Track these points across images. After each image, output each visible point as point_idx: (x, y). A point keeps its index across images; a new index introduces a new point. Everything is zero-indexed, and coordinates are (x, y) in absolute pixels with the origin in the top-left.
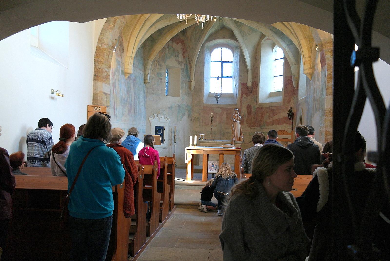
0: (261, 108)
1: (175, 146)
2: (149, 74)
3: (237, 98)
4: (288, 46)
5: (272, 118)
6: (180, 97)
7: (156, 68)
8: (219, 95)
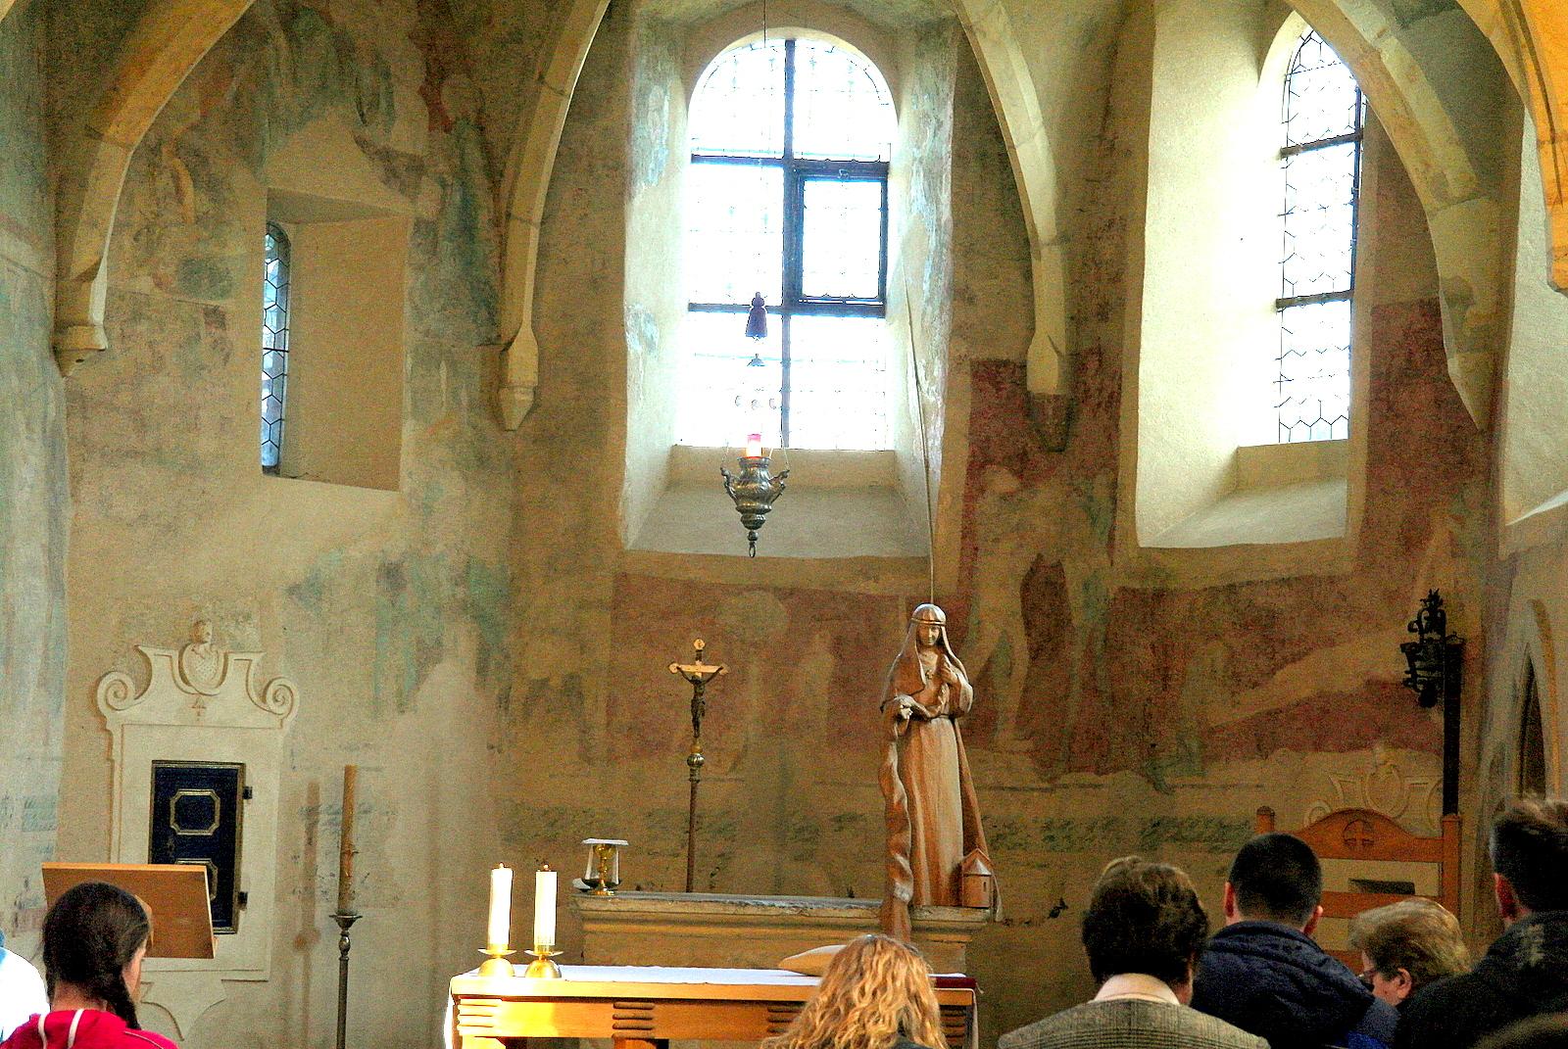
0: (1159, 595)
1: (345, 950)
2: (98, 264)
3: (934, 502)
4: (1405, 26)
5: (1255, 685)
6: (395, 487)
7: (169, 217)
8: (764, 473)
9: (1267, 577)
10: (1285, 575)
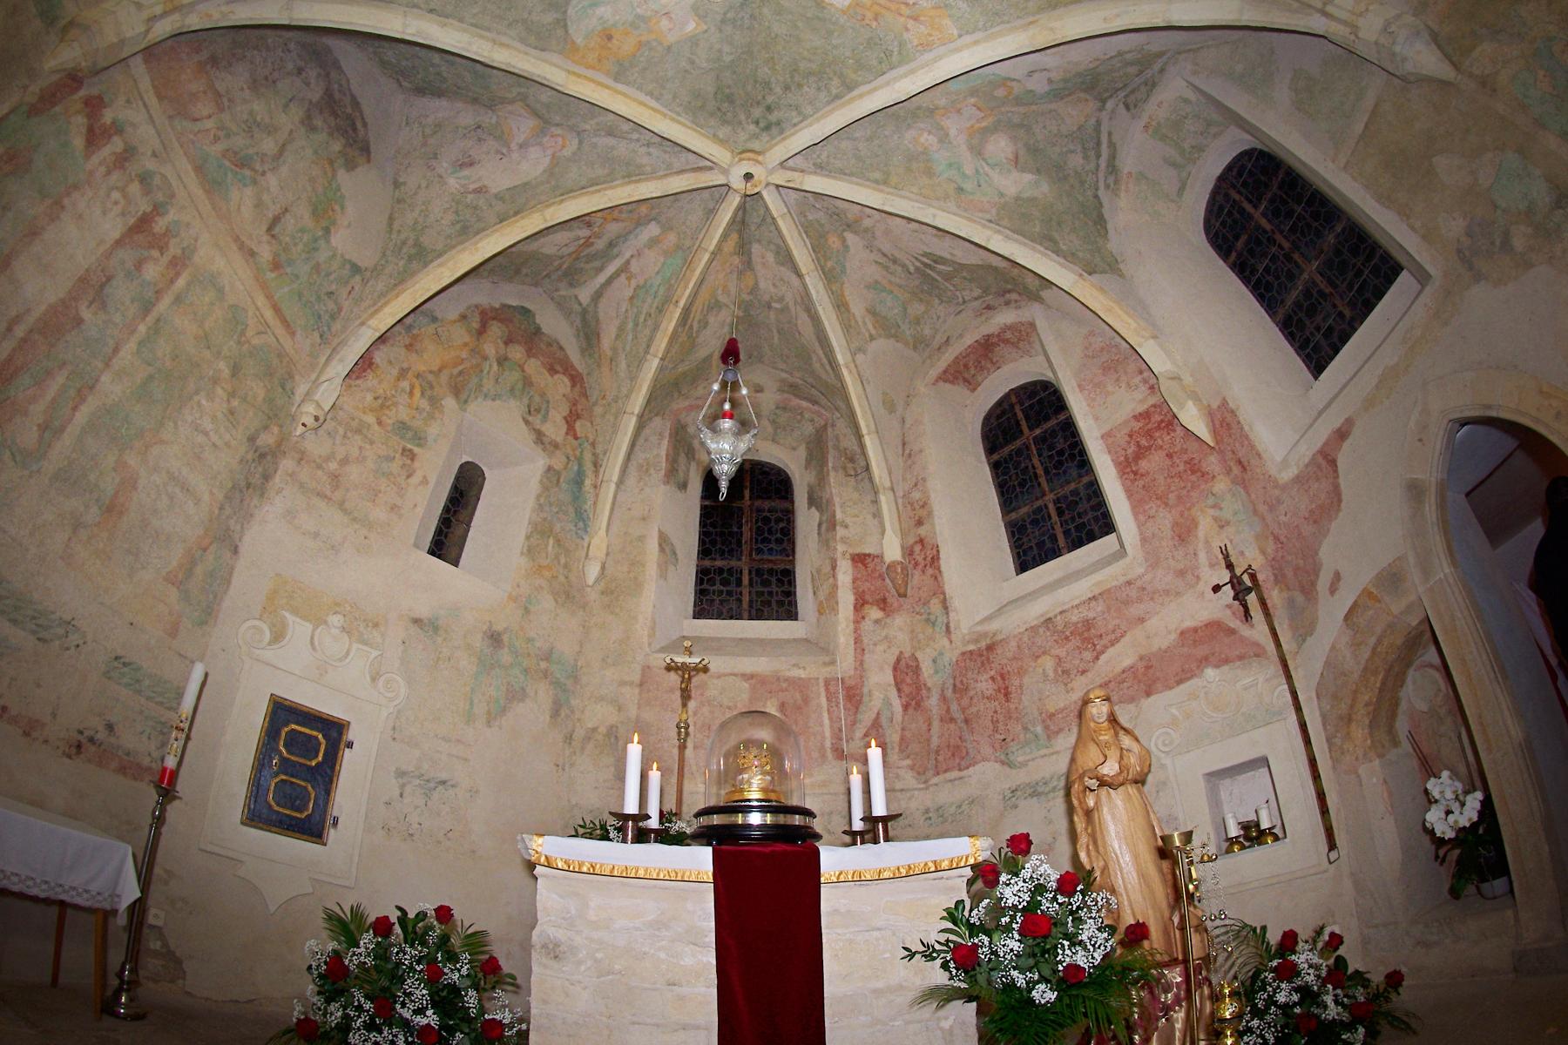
0: (990, 648)
5: (1084, 672)
9: (1076, 602)
10: (1090, 595)
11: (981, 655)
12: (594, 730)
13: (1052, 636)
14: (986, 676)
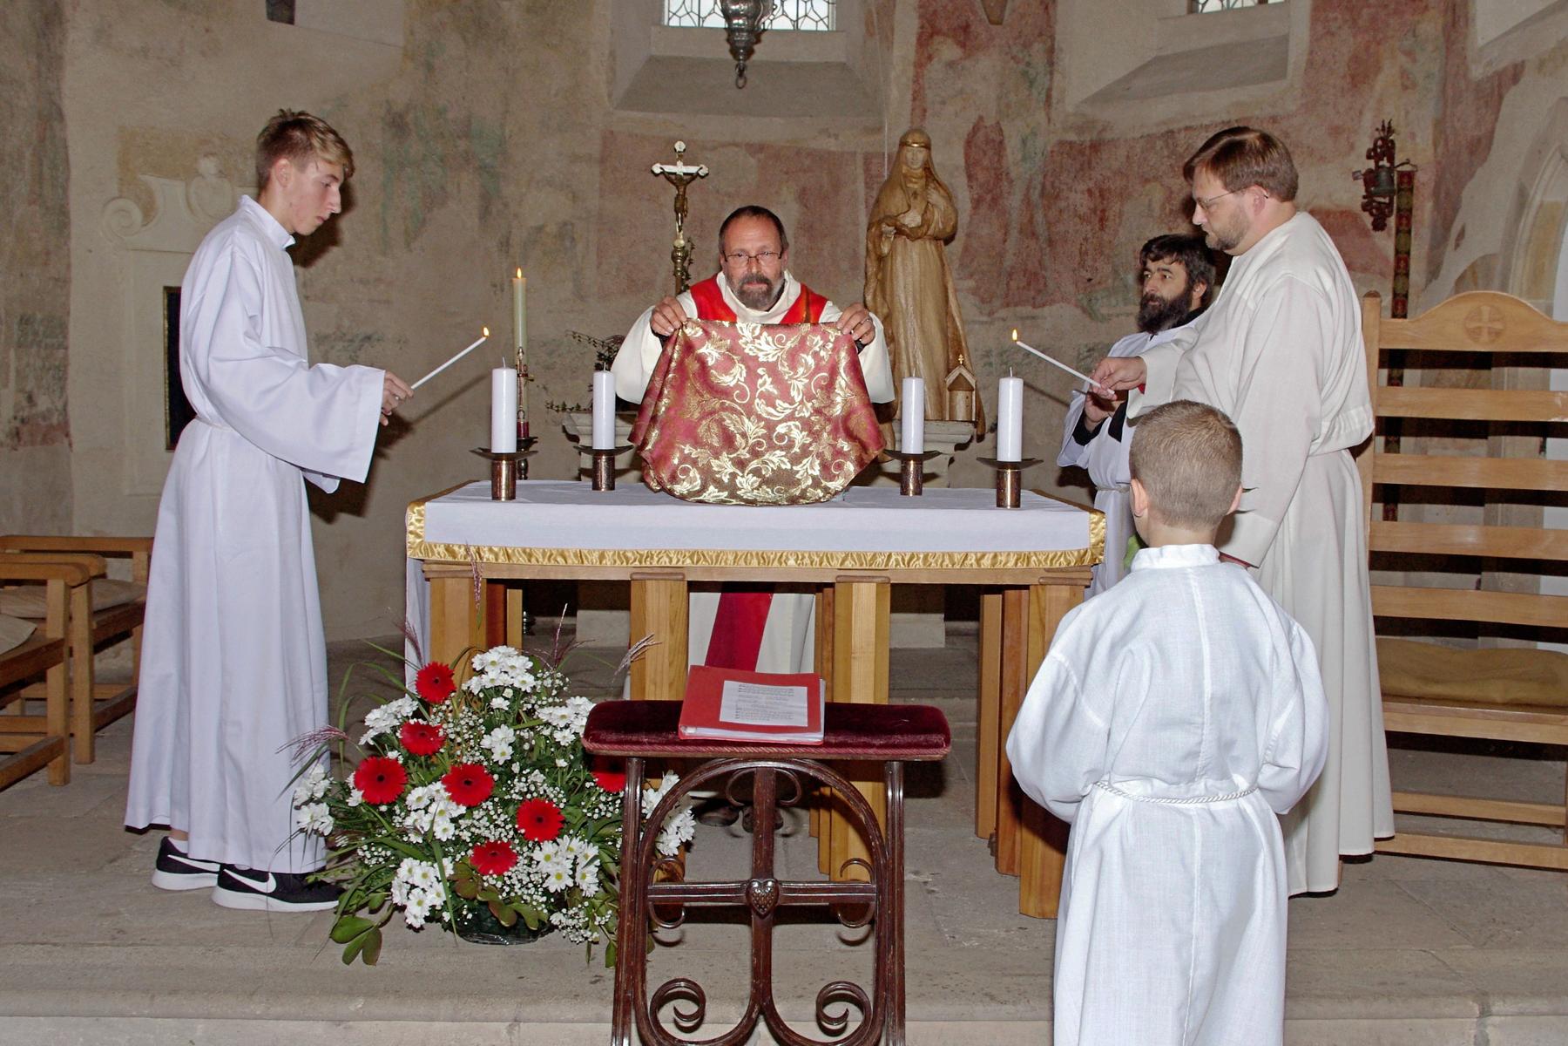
0: (1095, 147)
11: (1082, 153)
12: (540, 229)
13: (1169, 157)
14: (1082, 187)
